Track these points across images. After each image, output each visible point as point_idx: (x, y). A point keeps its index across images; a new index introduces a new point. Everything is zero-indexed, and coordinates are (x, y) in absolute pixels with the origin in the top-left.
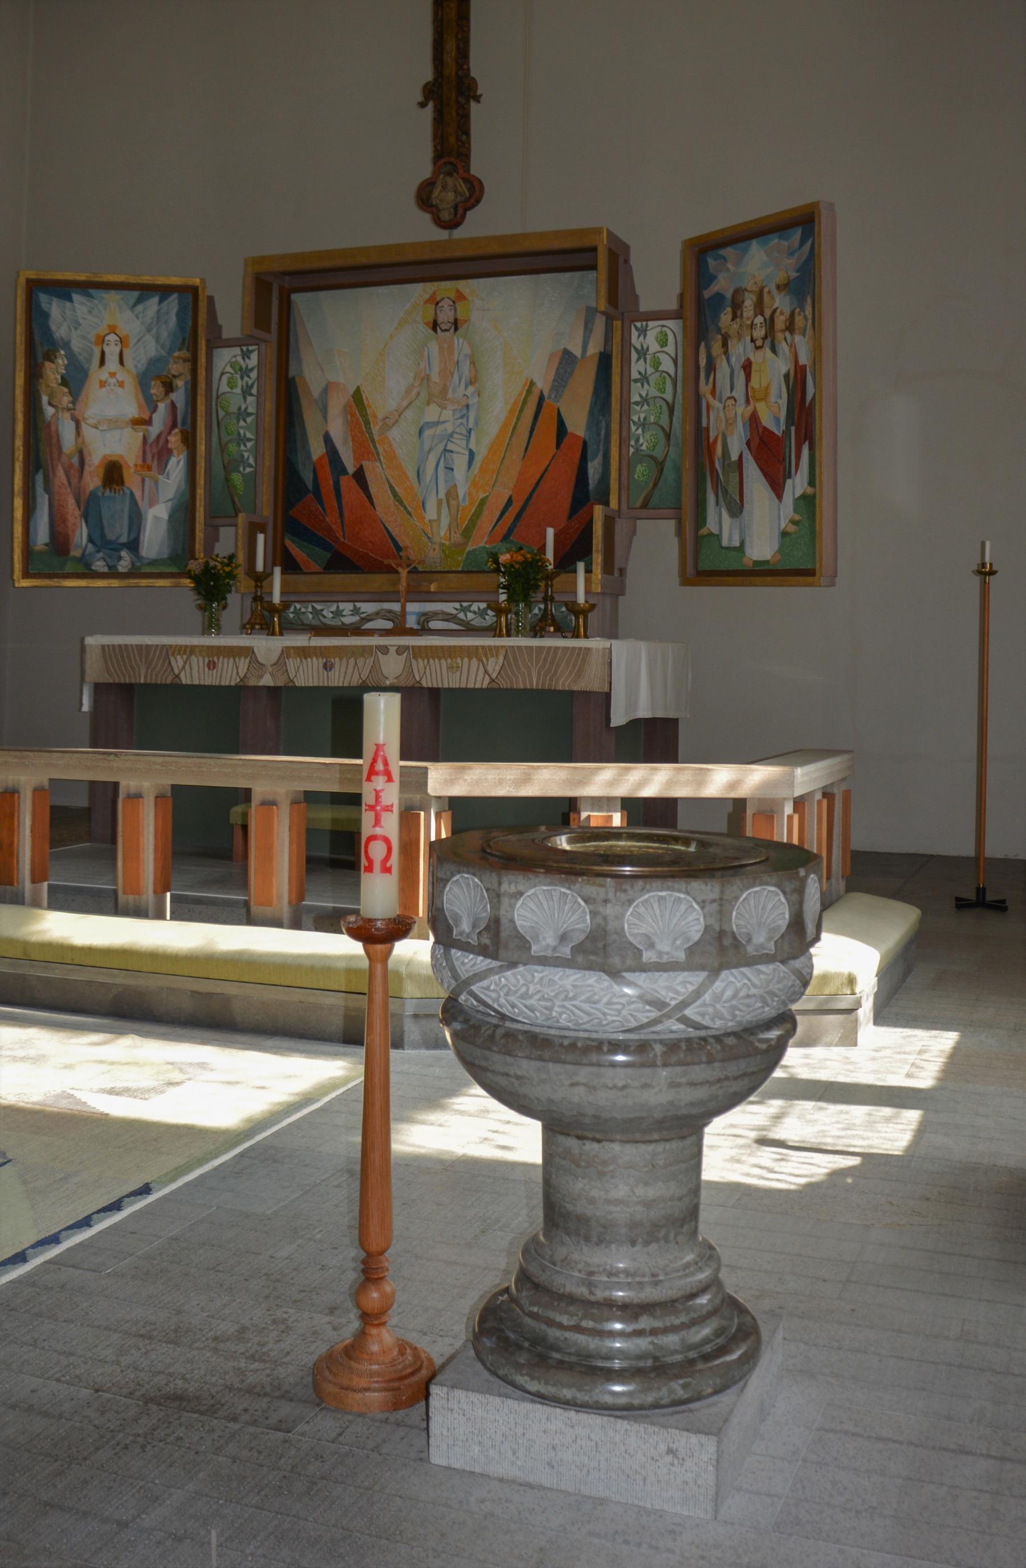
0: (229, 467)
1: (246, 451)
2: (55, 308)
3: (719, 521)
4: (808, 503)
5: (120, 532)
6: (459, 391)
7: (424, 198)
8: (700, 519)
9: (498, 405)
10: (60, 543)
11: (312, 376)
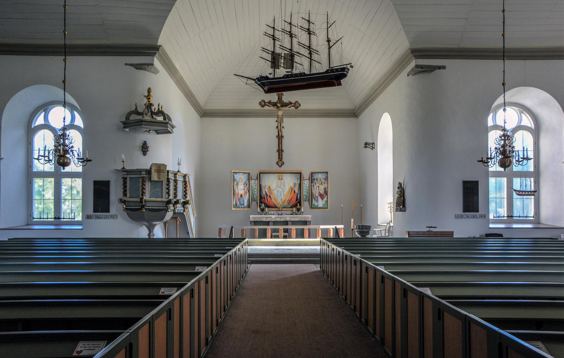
0: (253, 195)
1: (256, 193)
2: (235, 175)
3: (314, 202)
4: (327, 201)
5: (242, 203)
6: (282, 187)
7: (277, 163)
8: (312, 202)
9: (287, 188)
10: (236, 205)
11: (263, 184)
